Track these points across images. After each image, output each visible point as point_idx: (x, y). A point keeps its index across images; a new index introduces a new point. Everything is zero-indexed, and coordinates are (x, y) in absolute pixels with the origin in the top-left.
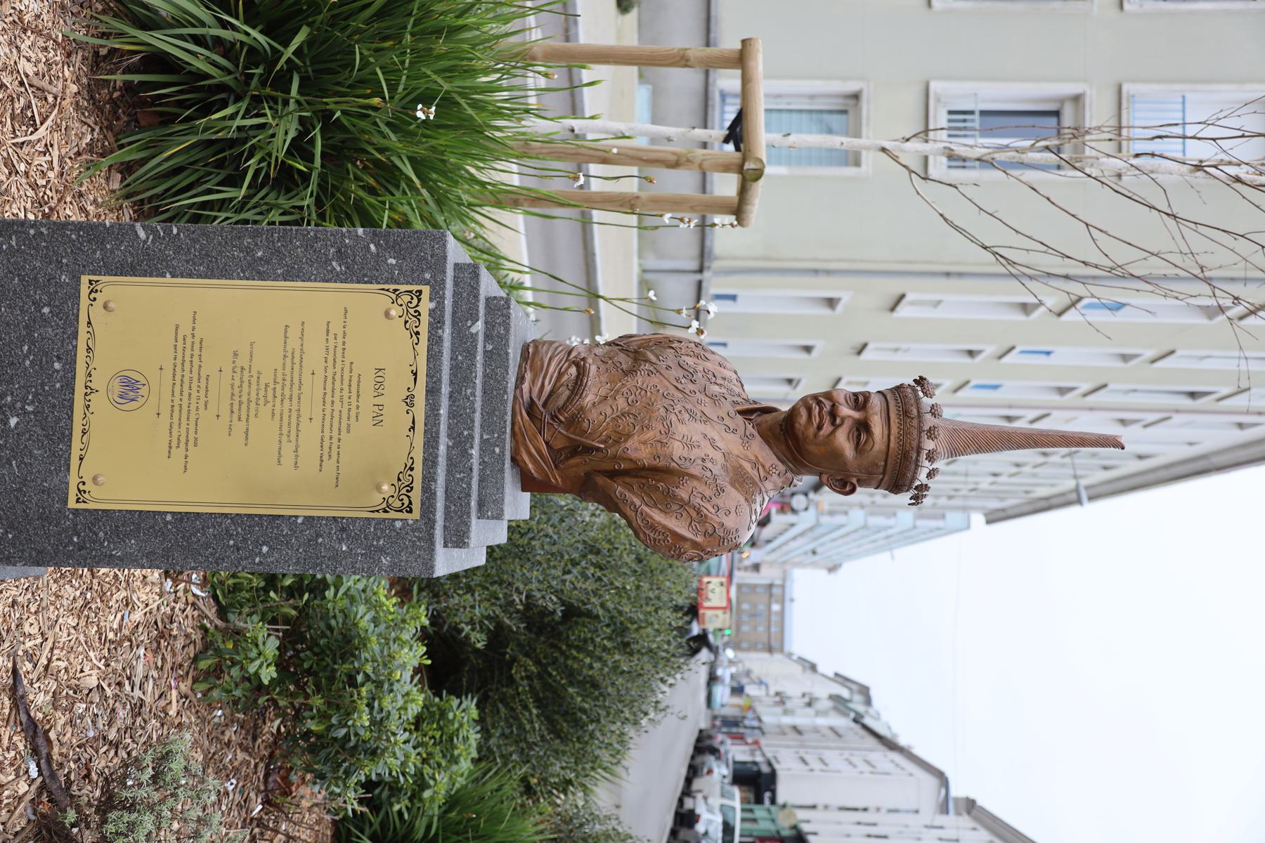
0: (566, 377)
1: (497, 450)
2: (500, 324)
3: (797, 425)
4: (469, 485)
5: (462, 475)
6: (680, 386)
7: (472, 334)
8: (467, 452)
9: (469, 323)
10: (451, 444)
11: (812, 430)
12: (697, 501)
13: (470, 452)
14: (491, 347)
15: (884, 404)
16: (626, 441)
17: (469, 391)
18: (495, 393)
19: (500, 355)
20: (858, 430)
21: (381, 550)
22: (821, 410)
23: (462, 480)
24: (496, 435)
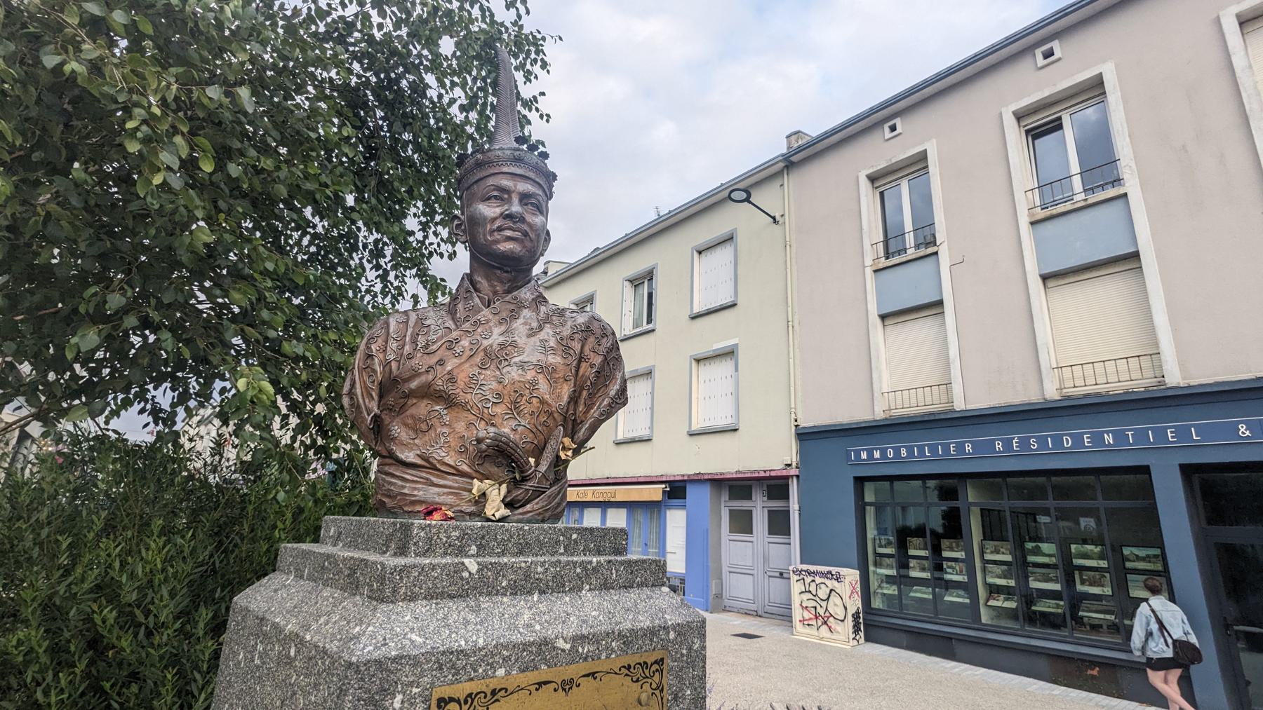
0: (465, 468)
1: (574, 536)
2: (448, 538)
3: (521, 254)
4: (622, 563)
5: (614, 571)
6: (468, 353)
7: (479, 570)
8: (594, 569)
9: (465, 574)
10: (588, 587)
11: (528, 244)
12: (602, 349)
13: (594, 565)
14: (474, 547)
15: (505, 176)
16: (549, 405)
17: (540, 569)
18: (521, 541)
19: (483, 537)
20: (526, 205)
21: (690, 649)
22: (510, 229)
23: (617, 571)
24: (561, 538)
